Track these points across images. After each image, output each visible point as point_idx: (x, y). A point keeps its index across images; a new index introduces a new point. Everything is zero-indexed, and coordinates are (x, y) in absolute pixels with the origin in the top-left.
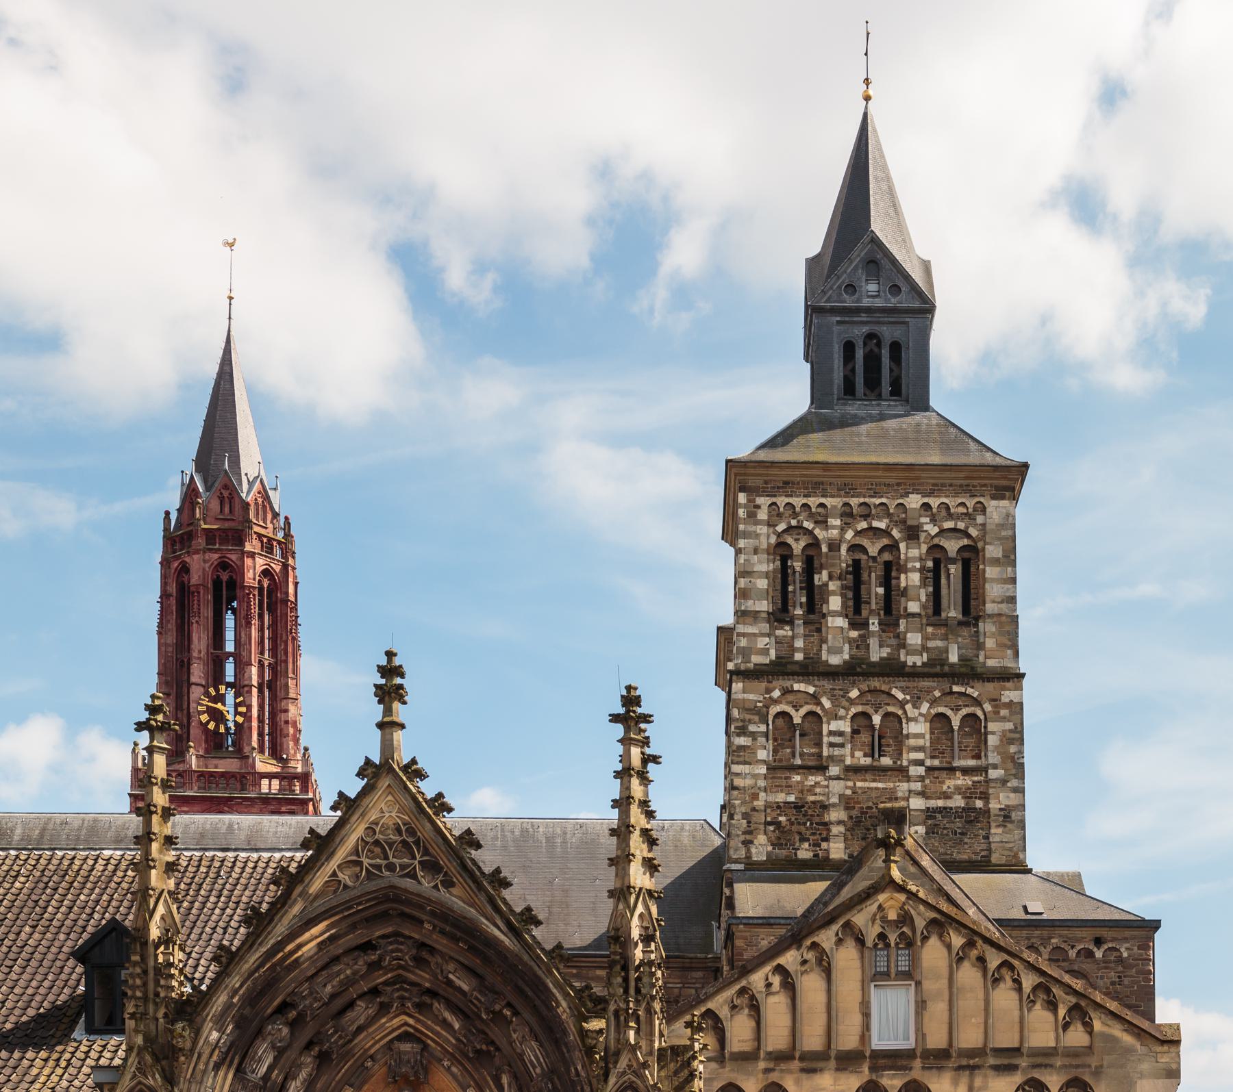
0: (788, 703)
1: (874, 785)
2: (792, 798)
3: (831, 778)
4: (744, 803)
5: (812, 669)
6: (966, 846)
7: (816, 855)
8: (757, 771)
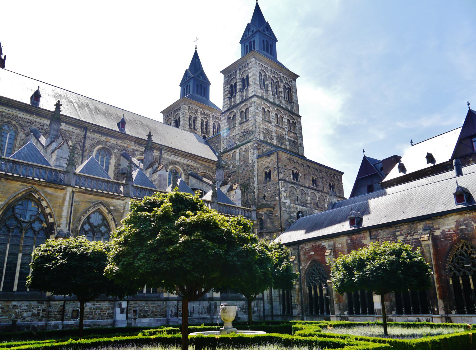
2: (266, 128)
3: (273, 126)
5: (267, 100)
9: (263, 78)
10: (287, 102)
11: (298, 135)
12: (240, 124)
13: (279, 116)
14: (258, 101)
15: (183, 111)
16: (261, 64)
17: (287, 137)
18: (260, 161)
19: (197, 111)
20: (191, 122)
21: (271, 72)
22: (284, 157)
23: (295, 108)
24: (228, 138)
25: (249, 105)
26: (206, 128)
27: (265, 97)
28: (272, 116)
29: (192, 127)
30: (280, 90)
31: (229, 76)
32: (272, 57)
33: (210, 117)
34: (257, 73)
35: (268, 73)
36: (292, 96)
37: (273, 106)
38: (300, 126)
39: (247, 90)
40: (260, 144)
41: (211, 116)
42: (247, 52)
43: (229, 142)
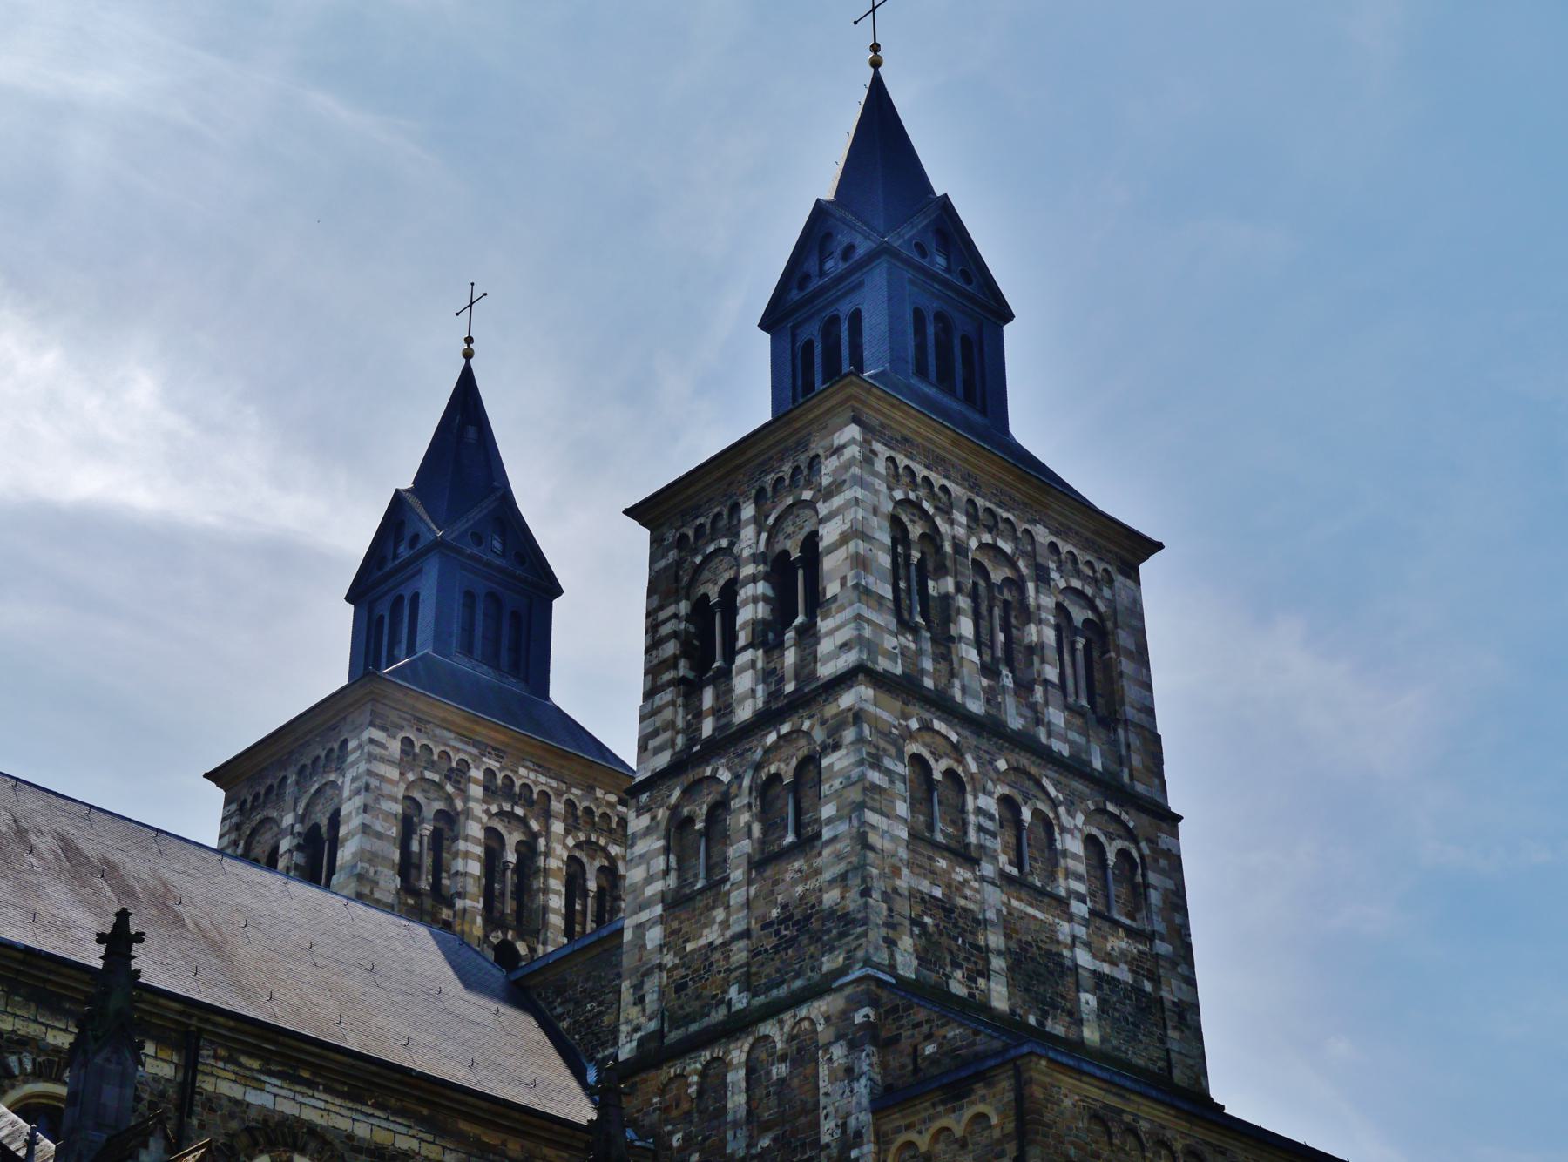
0: (926, 745)
1: (1031, 911)
2: (938, 893)
3: (983, 879)
4: (882, 875)
5: (942, 704)
6: (1141, 1047)
7: (971, 995)
8: (897, 832)
9: (916, 555)
10: (1078, 721)
11: (1163, 948)
12: (760, 863)
13: (1026, 814)
14: (886, 712)
15: (363, 766)
16: (902, 460)
17: (1083, 958)
18: (898, 1130)
19: (458, 775)
20: (415, 847)
21: (973, 515)
22: (1067, 1102)
23: (1136, 760)
24: (669, 959)
25: (819, 735)
26: (523, 891)
27: (929, 683)
28: (979, 811)
29: (425, 884)
30: (1032, 633)
31: (684, 537)
32: (975, 417)
33: (547, 815)
34: (875, 521)
35: (952, 522)
36: (1112, 676)
37: (984, 744)
38: (1170, 884)
39: (808, 635)
40: (895, 1009)
41: (558, 806)
42: (809, 387)
43: (680, 988)
